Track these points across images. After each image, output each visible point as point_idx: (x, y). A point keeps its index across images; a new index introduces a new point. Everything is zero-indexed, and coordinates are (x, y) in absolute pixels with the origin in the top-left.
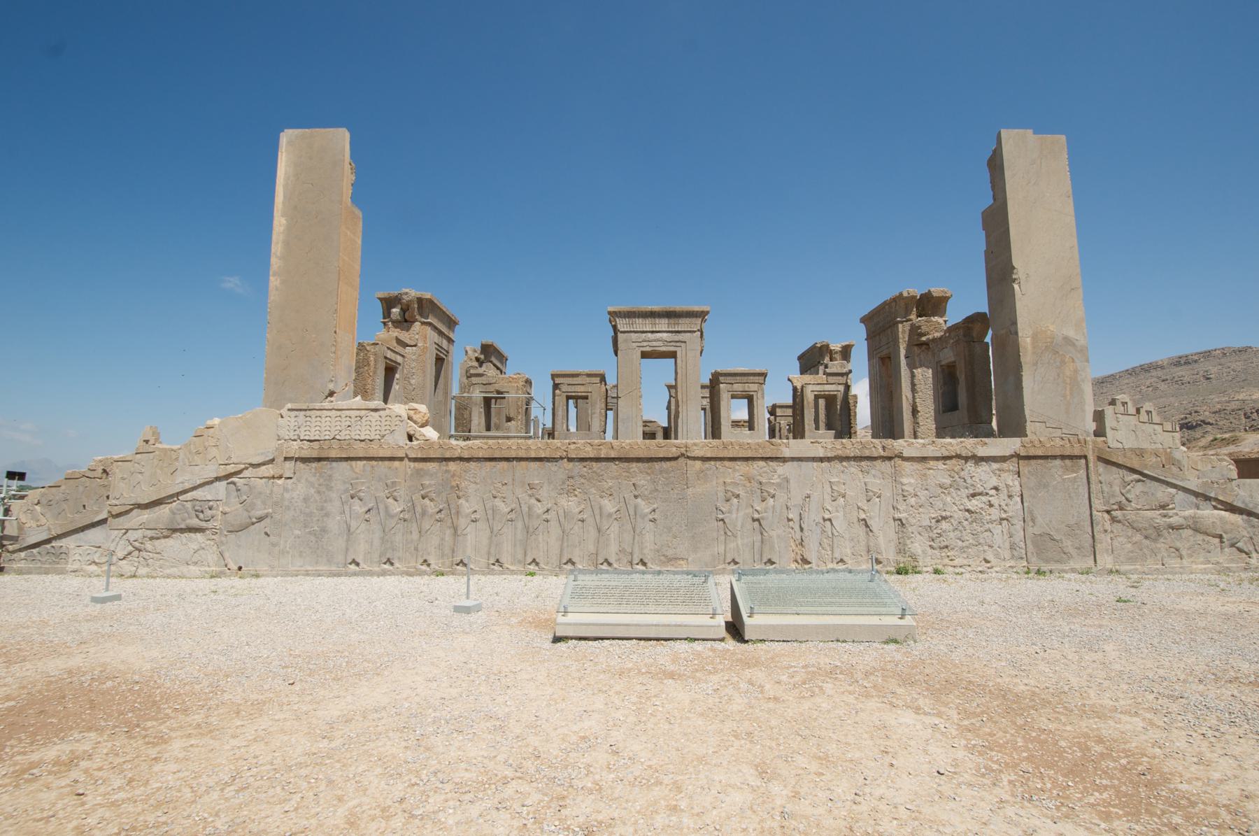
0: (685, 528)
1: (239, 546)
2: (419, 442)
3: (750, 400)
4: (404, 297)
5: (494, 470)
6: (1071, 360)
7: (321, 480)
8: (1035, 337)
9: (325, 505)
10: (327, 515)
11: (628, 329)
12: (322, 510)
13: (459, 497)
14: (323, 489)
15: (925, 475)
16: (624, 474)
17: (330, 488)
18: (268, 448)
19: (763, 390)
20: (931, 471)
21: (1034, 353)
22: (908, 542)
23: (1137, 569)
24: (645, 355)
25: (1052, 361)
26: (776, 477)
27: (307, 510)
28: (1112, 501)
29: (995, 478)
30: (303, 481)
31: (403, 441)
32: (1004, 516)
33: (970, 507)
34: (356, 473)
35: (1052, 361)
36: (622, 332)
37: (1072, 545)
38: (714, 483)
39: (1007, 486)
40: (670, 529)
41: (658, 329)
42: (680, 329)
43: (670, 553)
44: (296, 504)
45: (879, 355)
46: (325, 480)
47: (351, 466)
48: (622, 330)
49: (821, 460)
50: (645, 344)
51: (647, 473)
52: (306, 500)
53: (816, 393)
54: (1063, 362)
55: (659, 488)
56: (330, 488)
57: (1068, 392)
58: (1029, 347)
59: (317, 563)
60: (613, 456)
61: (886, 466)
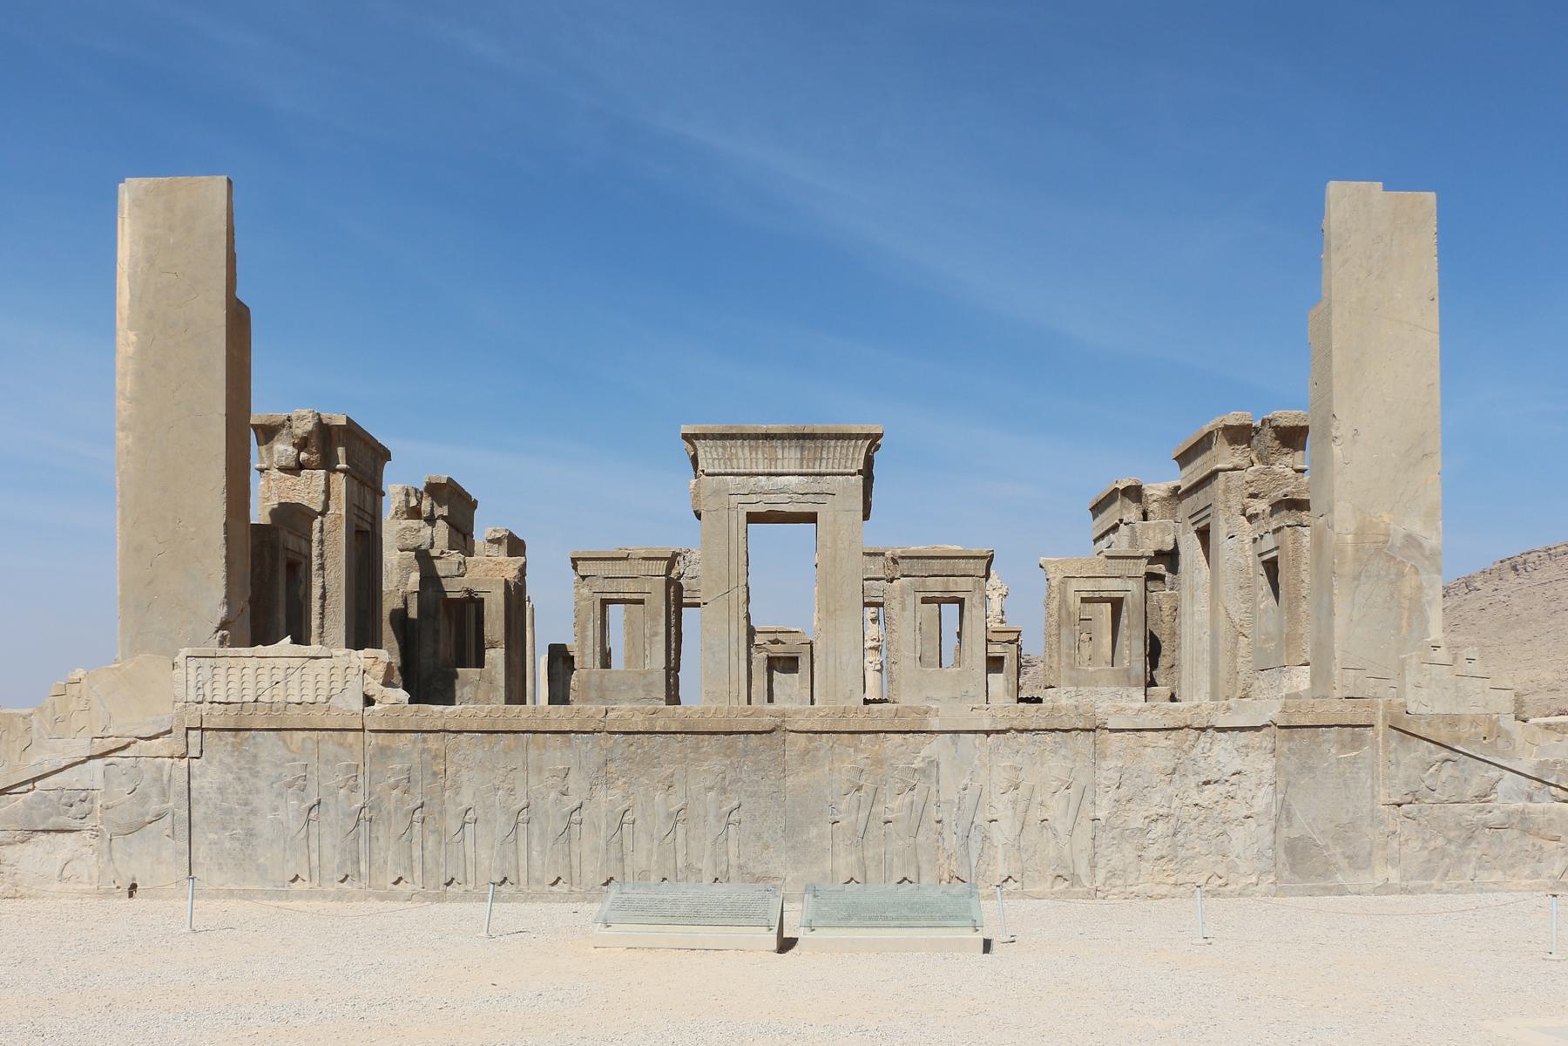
0: (781, 834)
1: (130, 855)
2: (383, 706)
3: (961, 602)
5: (495, 750)
6: (1413, 570)
7: (243, 762)
9: (250, 797)
10: (253, 812)
11: (723, 471)
12: (246, 804)
13: (443, 789)
14: (245, 774)
16: (692, 756)
17: (256, 775)
18: (164, 716)
19: (983, 590)
23: (1432, 885)
24: (753, 518)
26: (920, 759)
29: (1238, 760)
30: (215, 762)
31: (358, 704)
34: (292, 752)
36: (708, 475)
37: (1343, 853)
38: (827, 769)
40: (759, 837)
41: (779, 470)
42: (823, 470)
43: (759, 870)
44: (208, 796)
45: (1195, 527)
46: (248, 762)
47: (285, 742)
48: (710, 470)
49: (988, 733)
50: (754, 498)
51: (725, 755)
52: (221, 790)
53: (1085, 595)
55: (744, 776)
56: (256, 775)
57: (1404, 623)
59: (244, 881)
60: (674, 730)
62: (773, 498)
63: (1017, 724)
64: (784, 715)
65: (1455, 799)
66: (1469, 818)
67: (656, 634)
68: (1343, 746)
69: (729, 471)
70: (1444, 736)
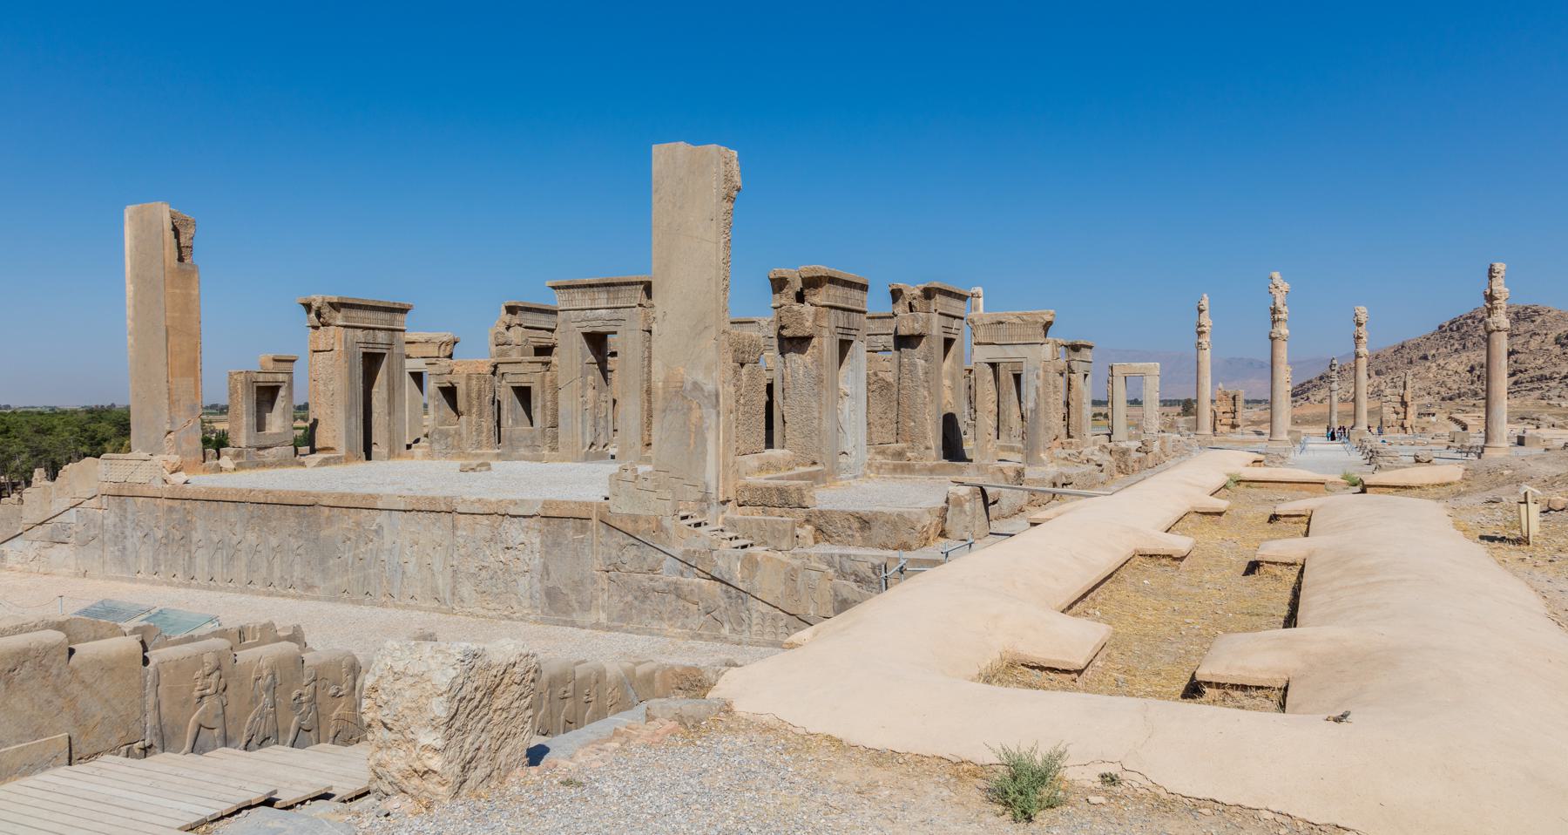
4: (313, 303)
8: (666, 382)
10: (125, 538)
14: (123, 518)
15: (474, 529)
17: (126, 518)
20: (478, 526)
21: (665, 399)
22: (458, 586)
25: (680, 408)
27: (116, 534)
28: (608, 563)
29: (522, 536)
32: (526, 569)
33: (502, 559)
35: (680, 408)
39: (532, 543)
41: (596, 307)
42: (619, 305)
50: (584, 324)
54: (690, 409)
57: (692, 442)
58: (660, 392)
61: (448, 518)
62: (594, 323)
63: (416, 507)
64: (318, 496)
65: (638, 570)
66: (644, 584)
67: (536, 407)
68: (577, 530)
69: (571, 308)
70: (630, 528)
